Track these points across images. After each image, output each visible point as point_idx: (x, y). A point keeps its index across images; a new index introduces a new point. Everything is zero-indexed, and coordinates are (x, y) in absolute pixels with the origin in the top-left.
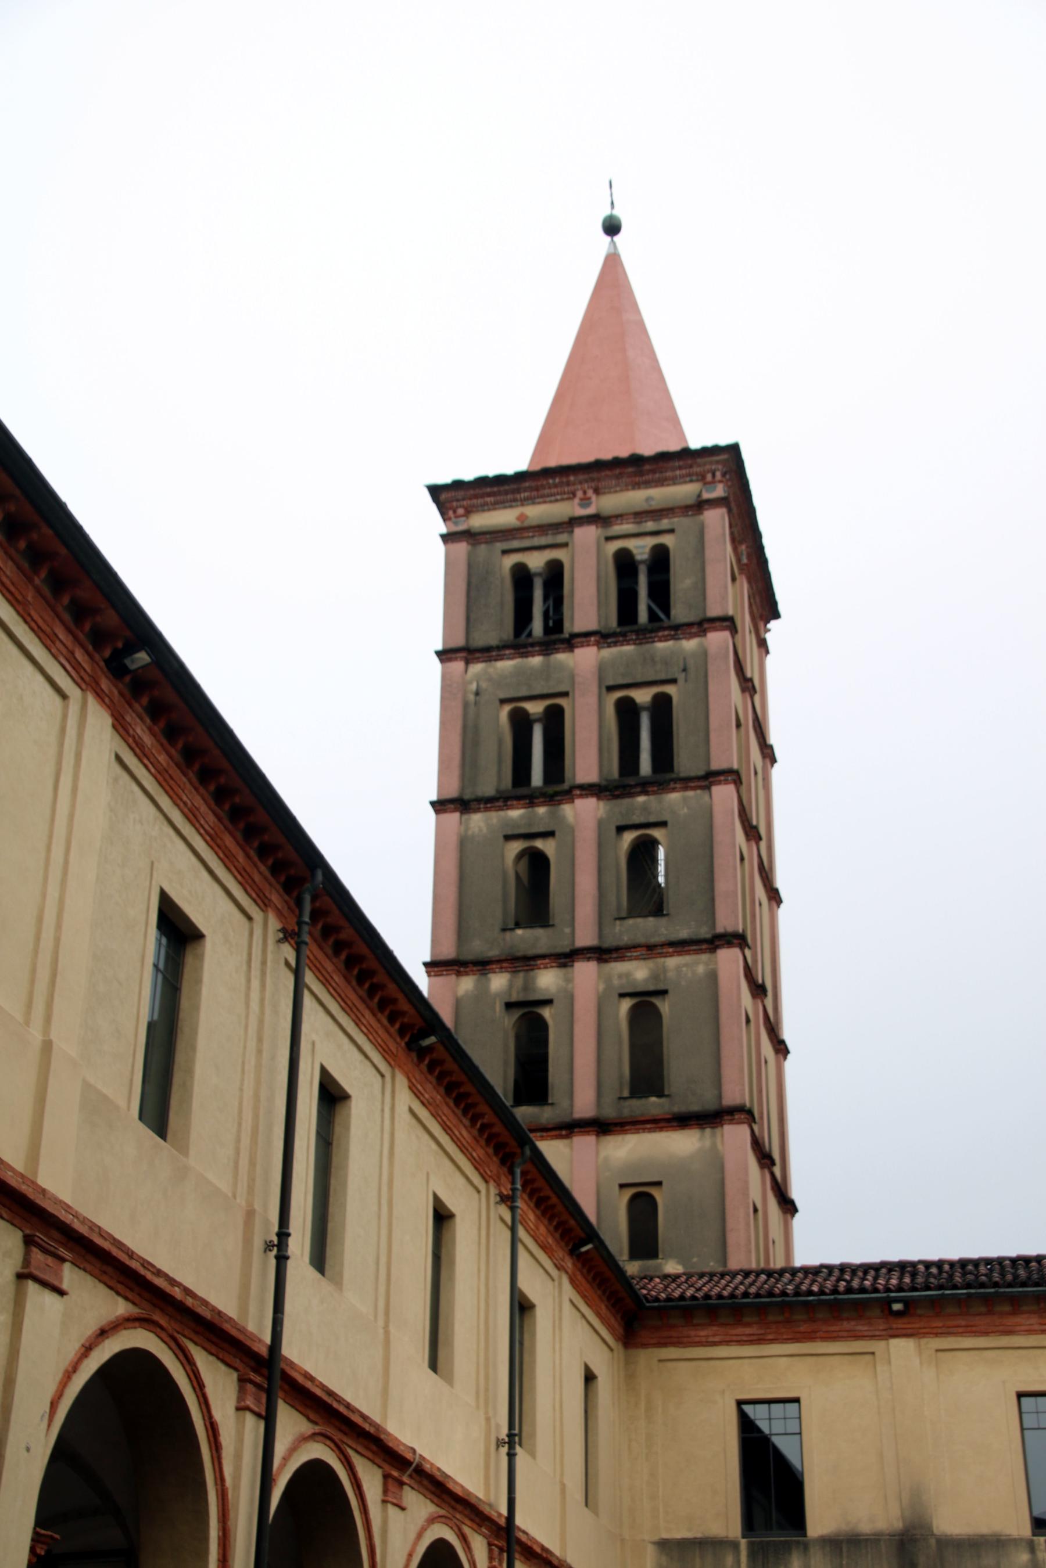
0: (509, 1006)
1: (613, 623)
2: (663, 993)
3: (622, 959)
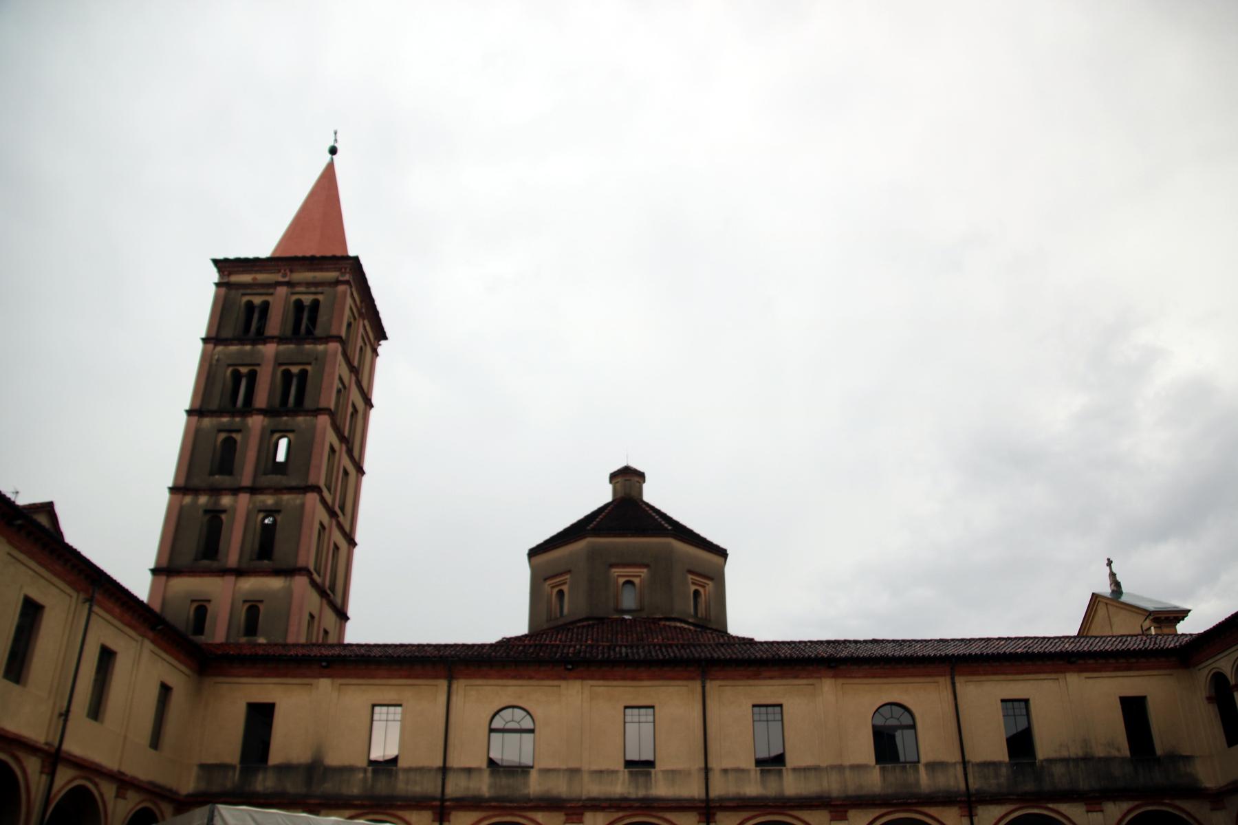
0: (206, 512)
1: (289, 333)
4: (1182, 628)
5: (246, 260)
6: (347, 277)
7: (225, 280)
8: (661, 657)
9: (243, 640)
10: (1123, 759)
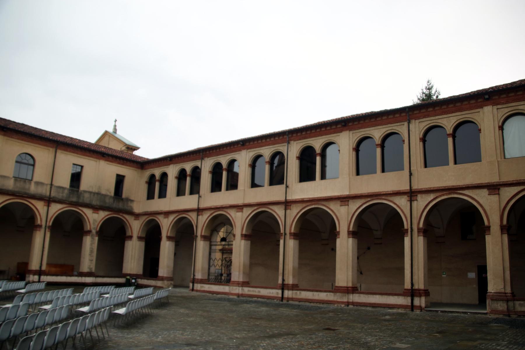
4: (136, 153)
10: (111, 197)
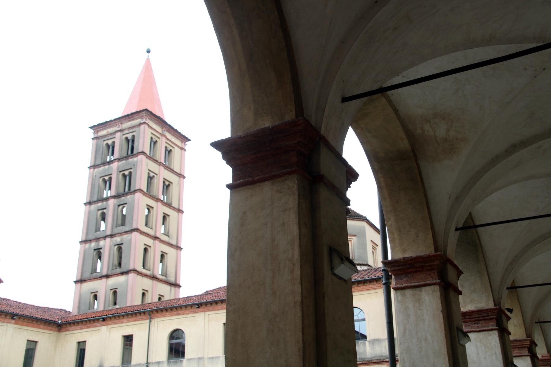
0: (95, 250)
2: (122, 244)
3: (115, 237)
5: (102, 124)
6: (144, 120)
7: (96, 136)
8: (205, 301)
9: (110, 308)
